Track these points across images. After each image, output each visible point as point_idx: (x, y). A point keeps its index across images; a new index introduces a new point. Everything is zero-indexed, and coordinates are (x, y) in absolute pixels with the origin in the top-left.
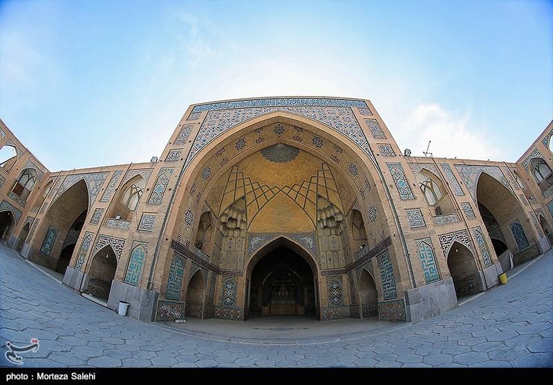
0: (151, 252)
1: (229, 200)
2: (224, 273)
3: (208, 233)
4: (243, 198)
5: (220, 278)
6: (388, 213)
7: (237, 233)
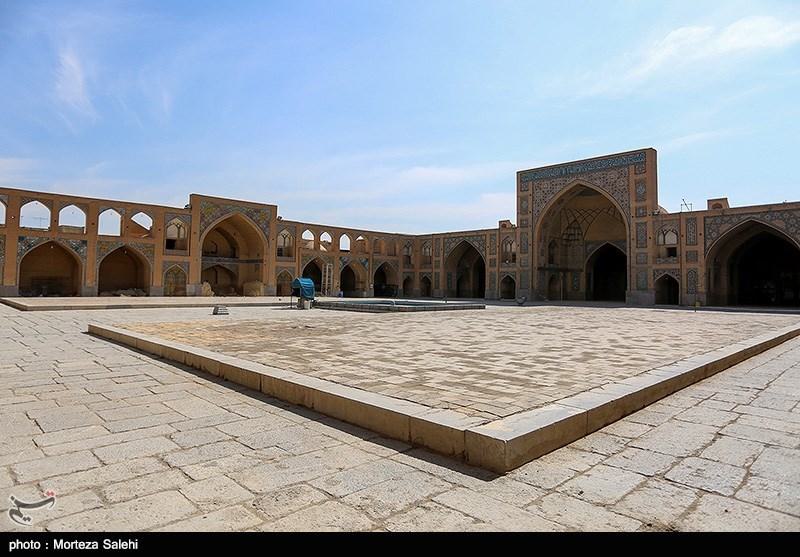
0: (530, 273)
1: (565, 224)
2: (572, 271)
3: (556, 249)
4: (575, 220)
5: (569, 274)
7: (576, 243)
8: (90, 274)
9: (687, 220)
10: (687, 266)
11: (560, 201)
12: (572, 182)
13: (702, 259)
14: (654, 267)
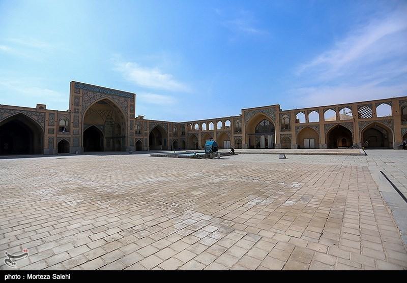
0: (80, 139)
6: (126, 132)
8: (357, 138)
9: (50, 114)
10: (145, 137)
11: (115, 106)
12: (104, 97)
13: (148, 135)
14: (136, 137)
